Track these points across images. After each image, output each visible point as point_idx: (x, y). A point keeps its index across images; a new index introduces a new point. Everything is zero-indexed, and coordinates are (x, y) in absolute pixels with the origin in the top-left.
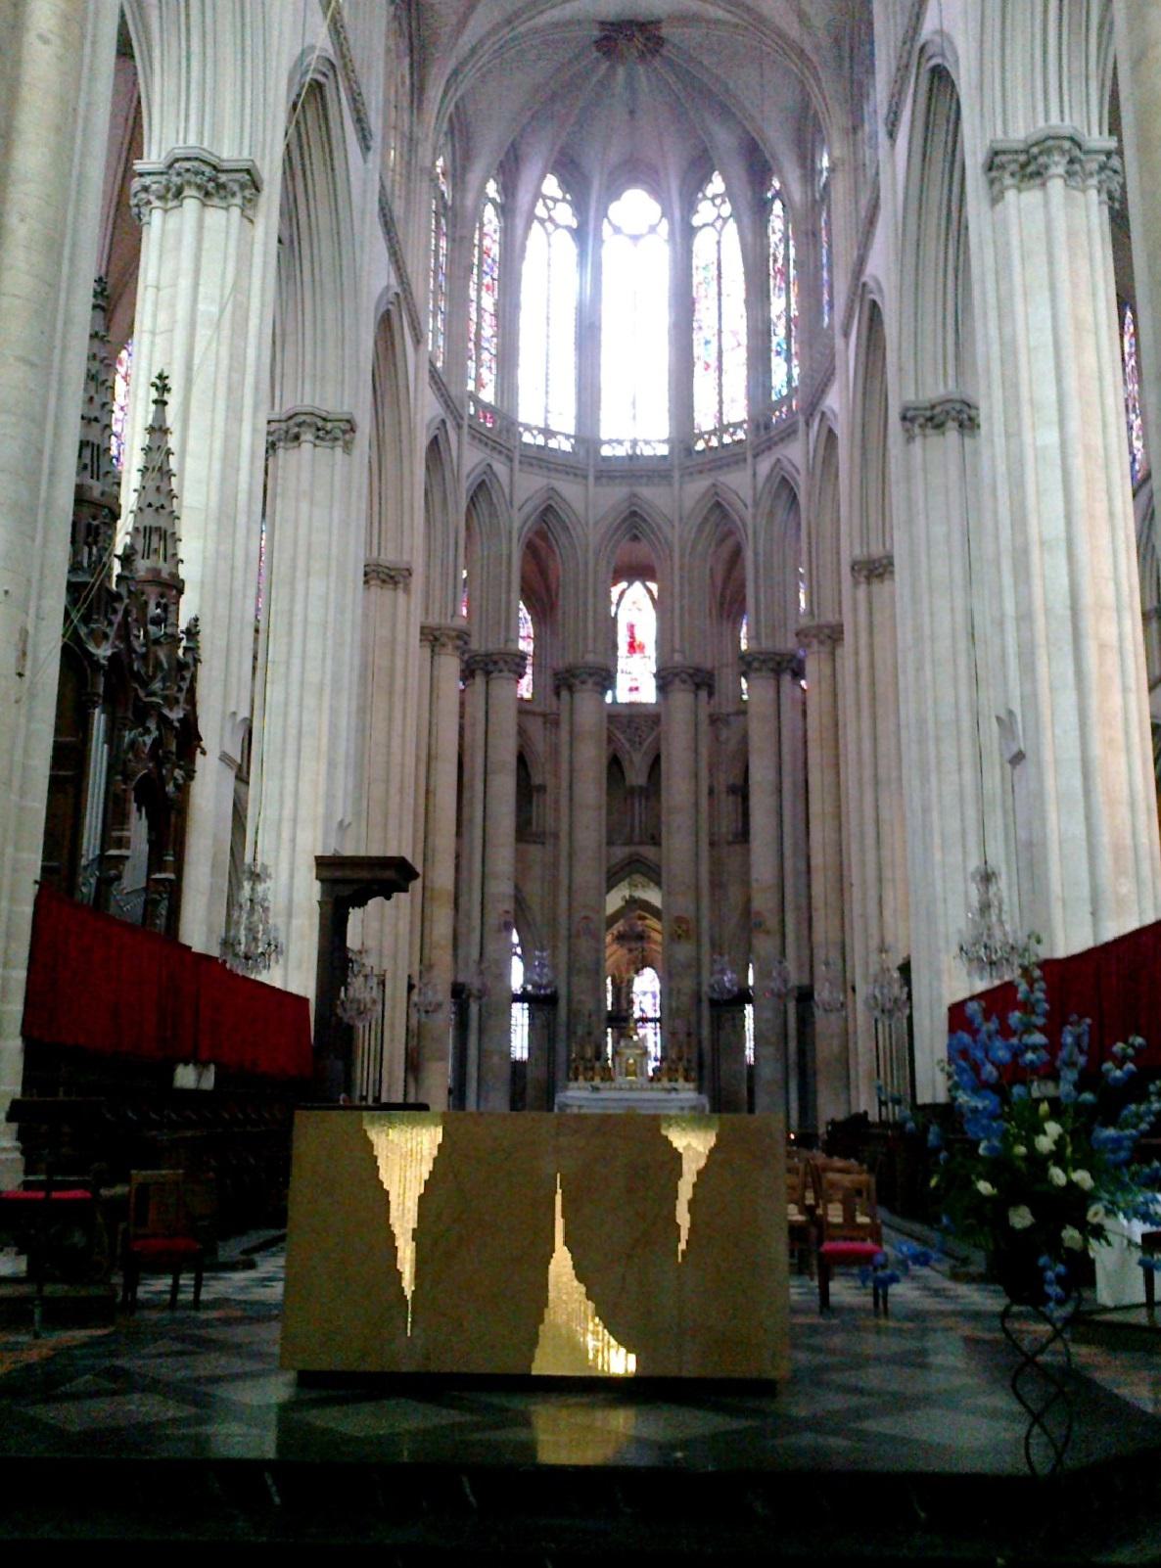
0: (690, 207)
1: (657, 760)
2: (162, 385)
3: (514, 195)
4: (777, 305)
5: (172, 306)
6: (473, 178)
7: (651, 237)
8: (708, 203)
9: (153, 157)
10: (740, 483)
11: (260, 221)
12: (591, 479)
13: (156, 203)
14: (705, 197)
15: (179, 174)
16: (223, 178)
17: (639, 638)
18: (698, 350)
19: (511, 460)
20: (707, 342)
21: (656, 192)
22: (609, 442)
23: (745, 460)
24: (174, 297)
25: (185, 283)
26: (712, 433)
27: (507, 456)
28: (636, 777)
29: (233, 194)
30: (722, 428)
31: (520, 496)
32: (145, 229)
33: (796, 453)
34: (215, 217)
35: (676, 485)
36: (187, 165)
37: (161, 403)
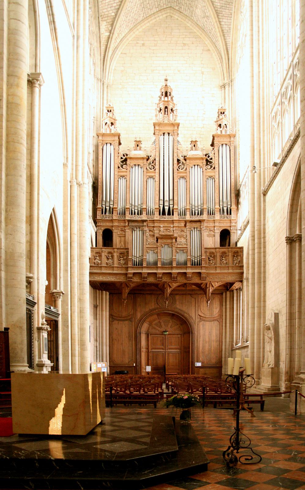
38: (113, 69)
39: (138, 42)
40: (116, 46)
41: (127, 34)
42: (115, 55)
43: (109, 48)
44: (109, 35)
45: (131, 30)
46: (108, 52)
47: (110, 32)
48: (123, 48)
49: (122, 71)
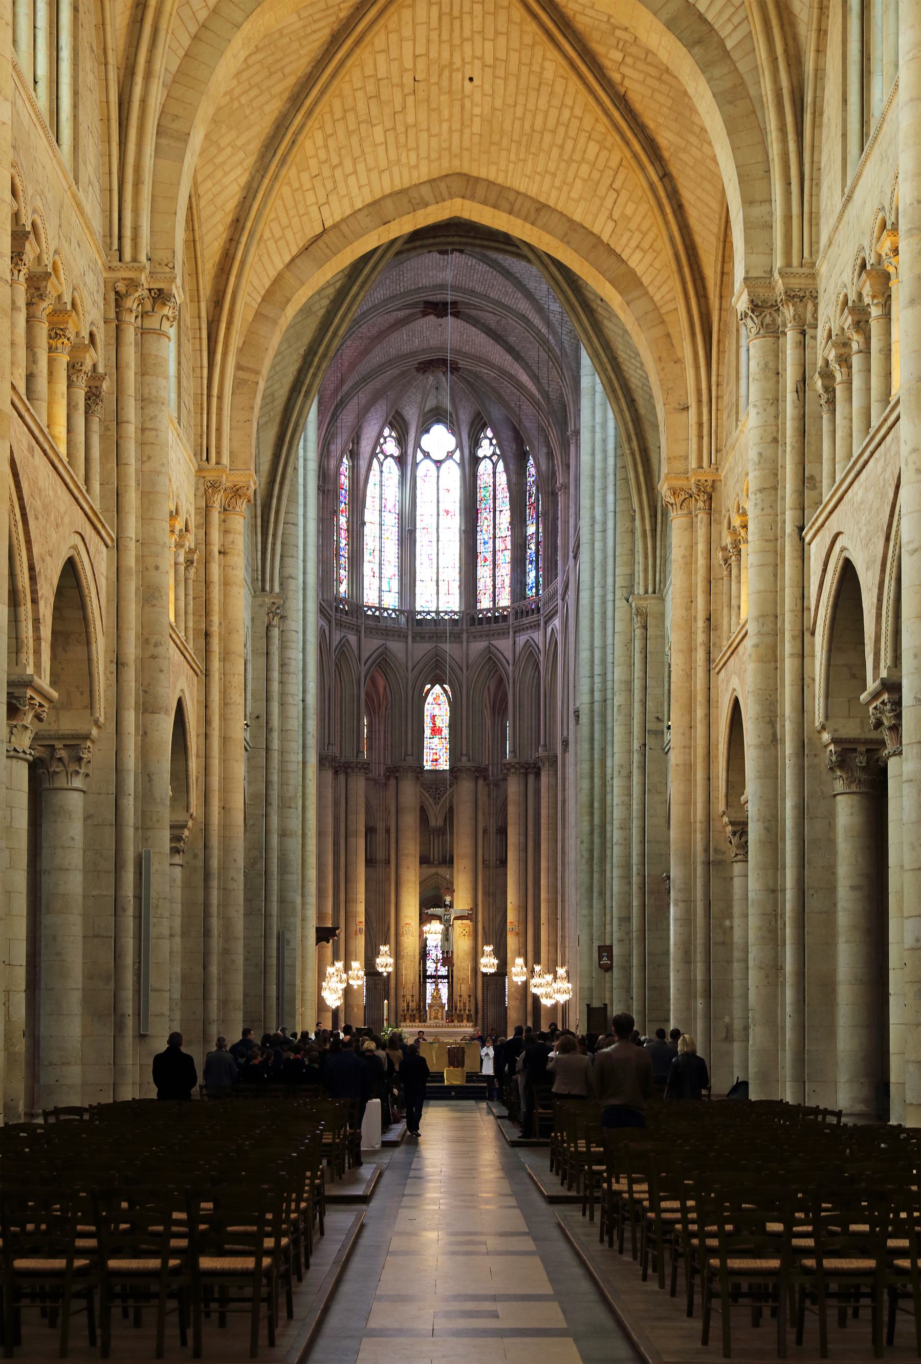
0: (475, 444)
1: (451, 809)
3: (358, 443)
4: (531, 529)
6: (336, 448)
10: (504, 645)
12: (410, 638)
14: (486, 437)
17: (439, 723)
18: (481, 548)
19: (358, 631)
21: (454, 429)
22: (420, 613)
26: (488, 610)
28: (435, 821)
30: (495, 608)
31: (365, 655)
33: (538, 637)
35: (465, 644)
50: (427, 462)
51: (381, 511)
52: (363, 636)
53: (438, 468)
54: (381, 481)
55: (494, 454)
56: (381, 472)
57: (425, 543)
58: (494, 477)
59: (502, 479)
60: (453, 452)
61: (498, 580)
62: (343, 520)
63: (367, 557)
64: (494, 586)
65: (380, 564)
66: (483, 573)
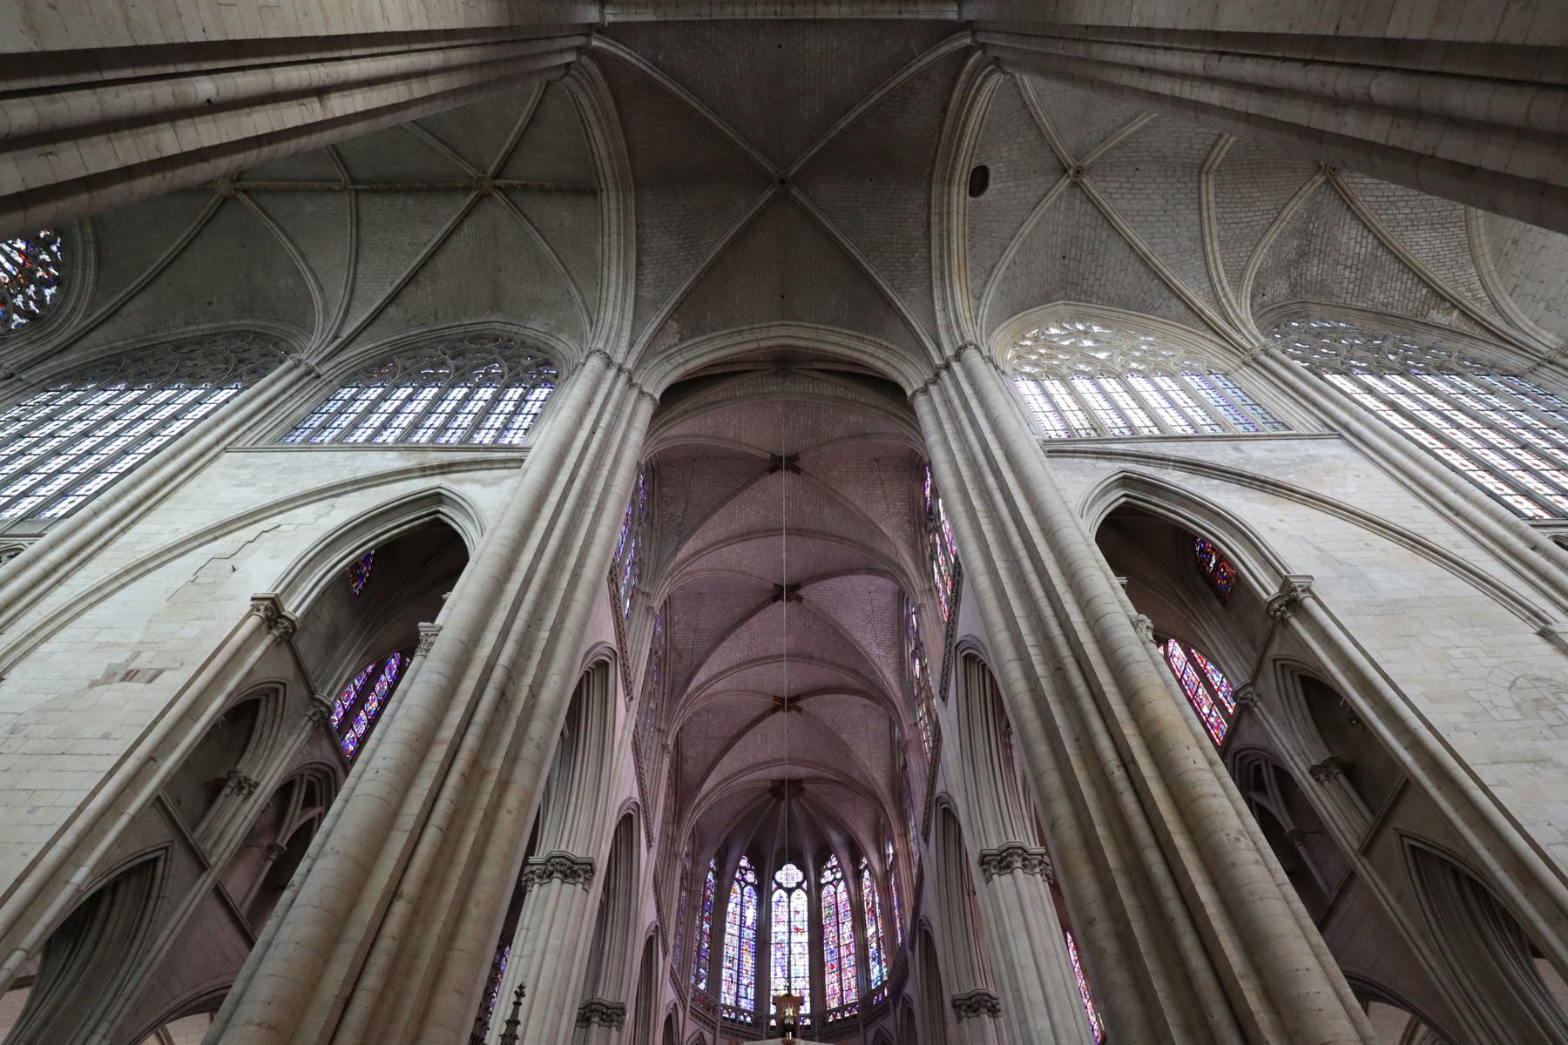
0: (819, 875)
2: (520, 994)
3: (724, 866)
4: (871, 931)
5: (535, 940)
7: (799, 891)
8: (829, 872)
9: (540, 856)
11: (592, 892)
13: (537, 880)
15: (552, 865)
16: (576, 867)
18: (827, 957)
19: (714, 1029)
20: (832, 952)
21: (801, 867)
23: (859, 1029)
24: (537, 935)
25: (545, 927)
26: (837, 1010)
27: (713, 1027)
29: (580, 876)
30: (842, 1007)
32: (528, 894)
33: (889, 1023)
34: (567, 888)
36: (558, 860)
37: (517, 1004)
38: (1531, 324)
39: (1504, 253)
40: (1489, 302)
41: (1477, 271)
42: (1507, 310)
43: (1483, 319)
44: (1461, 311)
45: (1474, 261)
46: (1491, 325)
47: (1455, 307)
48: (1501, 288)
49: (1548, 308)
50: (781, 892)
51: (740, 926)
52: (718, 1034)
53: (789, 897)
54: (742, 902)
55: (835, 879)
56: (742, 895)
57: (779, 955)
58: (836, 897)
59: (843, 897)
60: (802, 882)
61: (845, 984)
62: (706, 926)
63: (726, 964)
64: (841, 990)
65: (738, 972)
66: (831, 979)
